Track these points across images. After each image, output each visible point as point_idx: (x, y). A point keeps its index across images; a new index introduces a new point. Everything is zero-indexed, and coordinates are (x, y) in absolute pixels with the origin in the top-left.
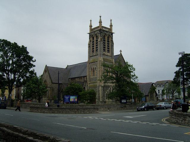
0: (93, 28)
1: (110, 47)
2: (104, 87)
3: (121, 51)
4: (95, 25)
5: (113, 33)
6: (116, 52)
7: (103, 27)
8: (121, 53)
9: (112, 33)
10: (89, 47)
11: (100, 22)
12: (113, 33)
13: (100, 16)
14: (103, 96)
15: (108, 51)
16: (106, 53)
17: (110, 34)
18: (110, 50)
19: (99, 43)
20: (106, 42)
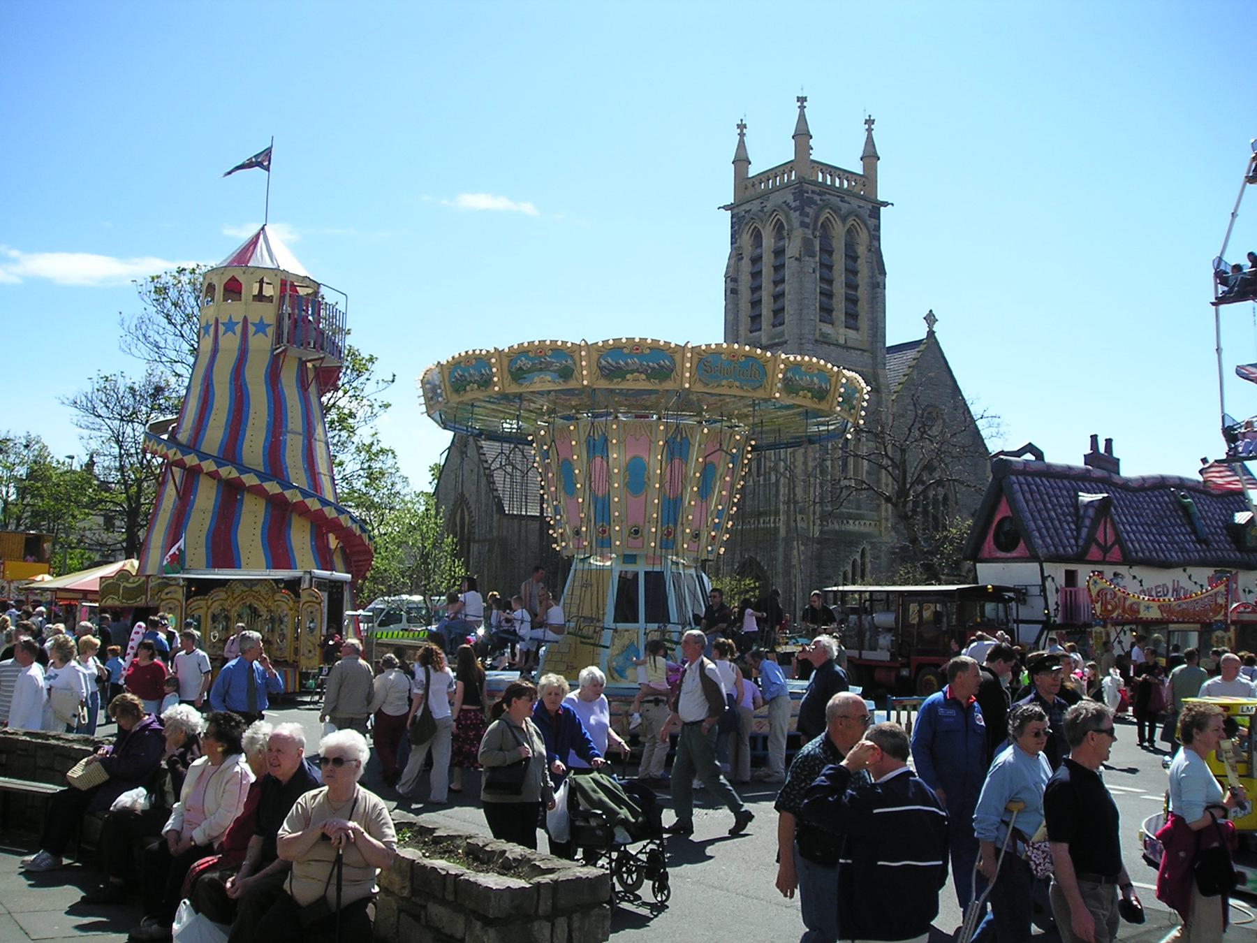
0: (753, 171)
1: (863, 292)
3: (930, 319)
4: (771, 152)
5: (885, 204)
6: (901, 327)
8: (931, 334)
9: (876, 208)
10: (732, 292)
11: (802, 135)
12: (885, 204)
13: (802, 100)
15: (852, 319)
16: (841, 333)
17: (865, 213)
18: (863, 308)
19: (791, 267)
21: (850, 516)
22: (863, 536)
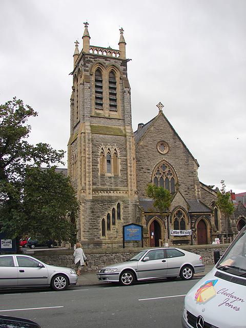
2: (94, 201)
3: (160, 105)
7: (93, 48)
8: (161, 111)
9: (125, 62)
12: (128, 60)
13: (86, 24)
14: (93, 226)
15: (113, 107)
16: (106, 112)
17: (118, 64)
18: (119, 103)
20: (106, 85)
21: (111, 190)
22: (118, 198)
